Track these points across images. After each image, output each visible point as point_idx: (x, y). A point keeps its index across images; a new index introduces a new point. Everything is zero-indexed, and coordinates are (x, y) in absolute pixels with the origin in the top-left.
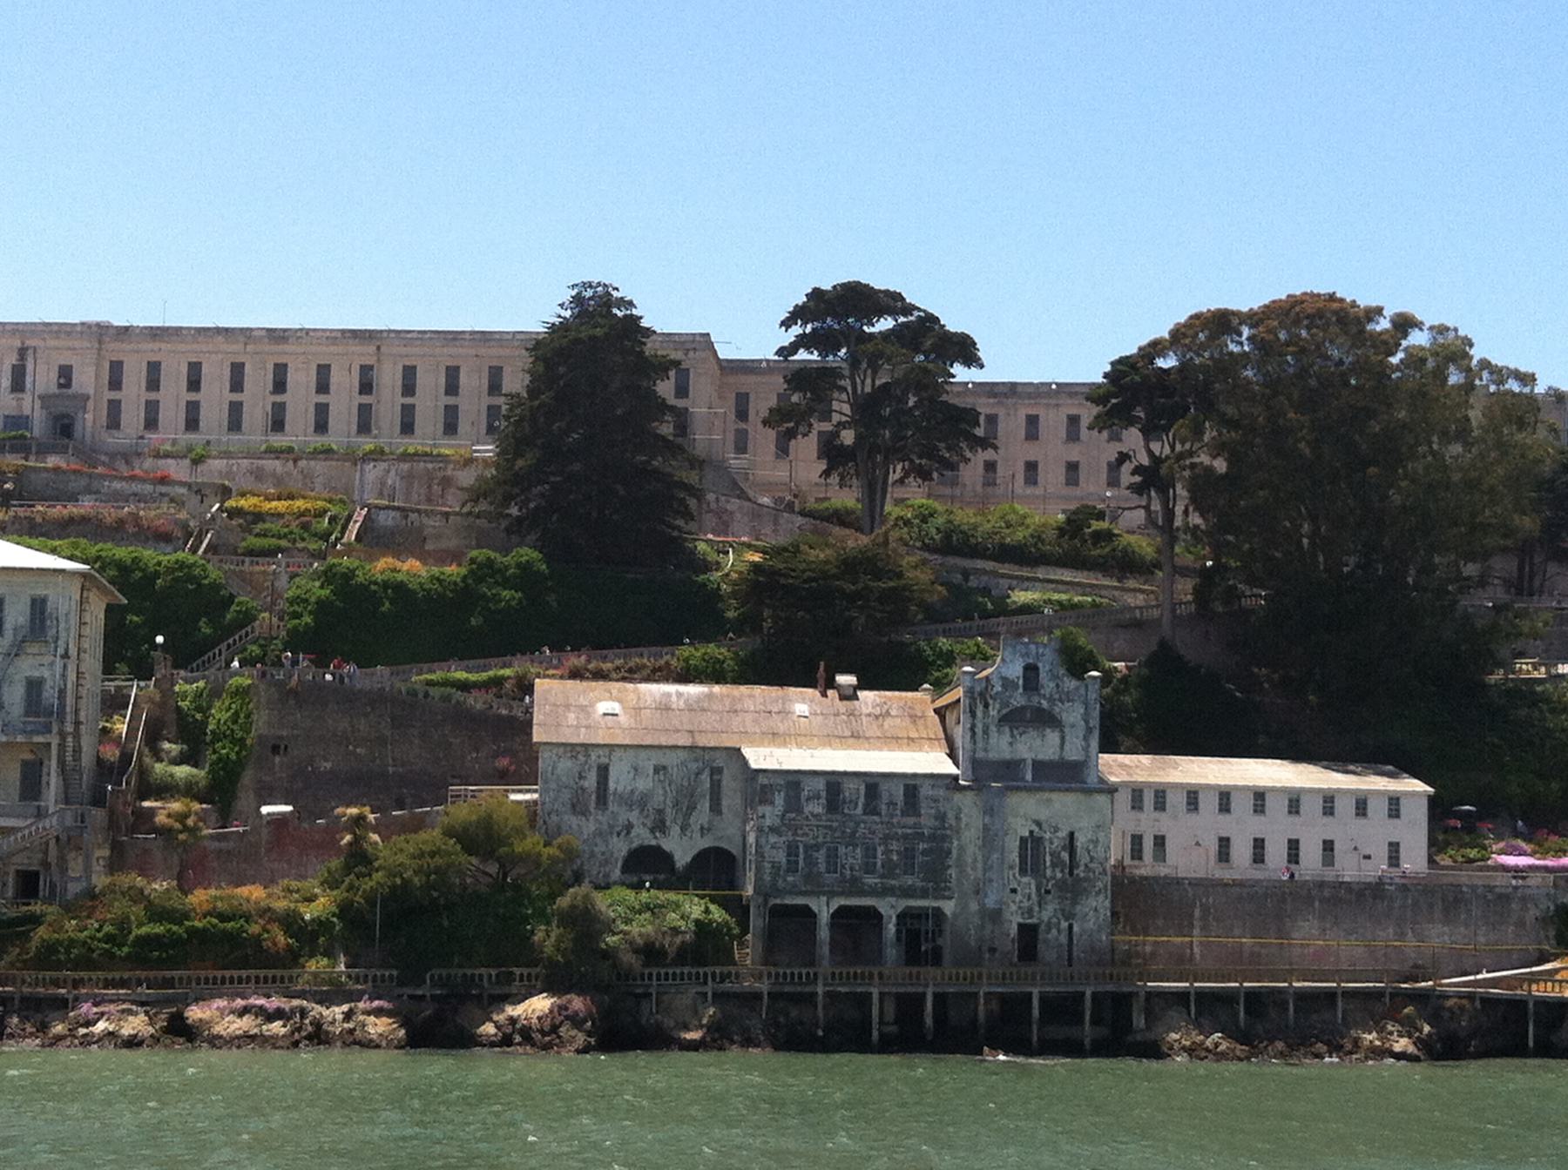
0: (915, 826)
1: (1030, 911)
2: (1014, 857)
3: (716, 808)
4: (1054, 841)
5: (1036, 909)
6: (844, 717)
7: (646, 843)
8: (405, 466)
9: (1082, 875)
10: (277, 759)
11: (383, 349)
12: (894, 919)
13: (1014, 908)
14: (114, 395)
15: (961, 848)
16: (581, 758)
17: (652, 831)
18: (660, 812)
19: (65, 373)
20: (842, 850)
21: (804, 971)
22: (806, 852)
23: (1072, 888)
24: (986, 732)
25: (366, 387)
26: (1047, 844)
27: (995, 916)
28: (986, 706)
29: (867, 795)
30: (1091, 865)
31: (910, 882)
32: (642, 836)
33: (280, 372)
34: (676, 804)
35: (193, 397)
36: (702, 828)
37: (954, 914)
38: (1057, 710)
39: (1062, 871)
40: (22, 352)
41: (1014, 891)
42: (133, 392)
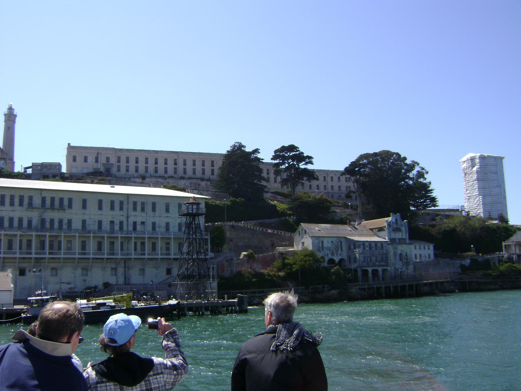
3: (341, 250)
4: (404, 254)
8: (190, 181)
10: (231, 243)
11: (179, 156)
14: (119, 164)
16: (319, 239)
17: (332, 255)
18: (333, 251)
19: (108, 159)
20: (372, 257)
23: (407, 264)
25: (175, 164)
32: (330, 256)
33: (156, 160)
35: (137, 165)
40: (98, 154)
42: (123, 164)
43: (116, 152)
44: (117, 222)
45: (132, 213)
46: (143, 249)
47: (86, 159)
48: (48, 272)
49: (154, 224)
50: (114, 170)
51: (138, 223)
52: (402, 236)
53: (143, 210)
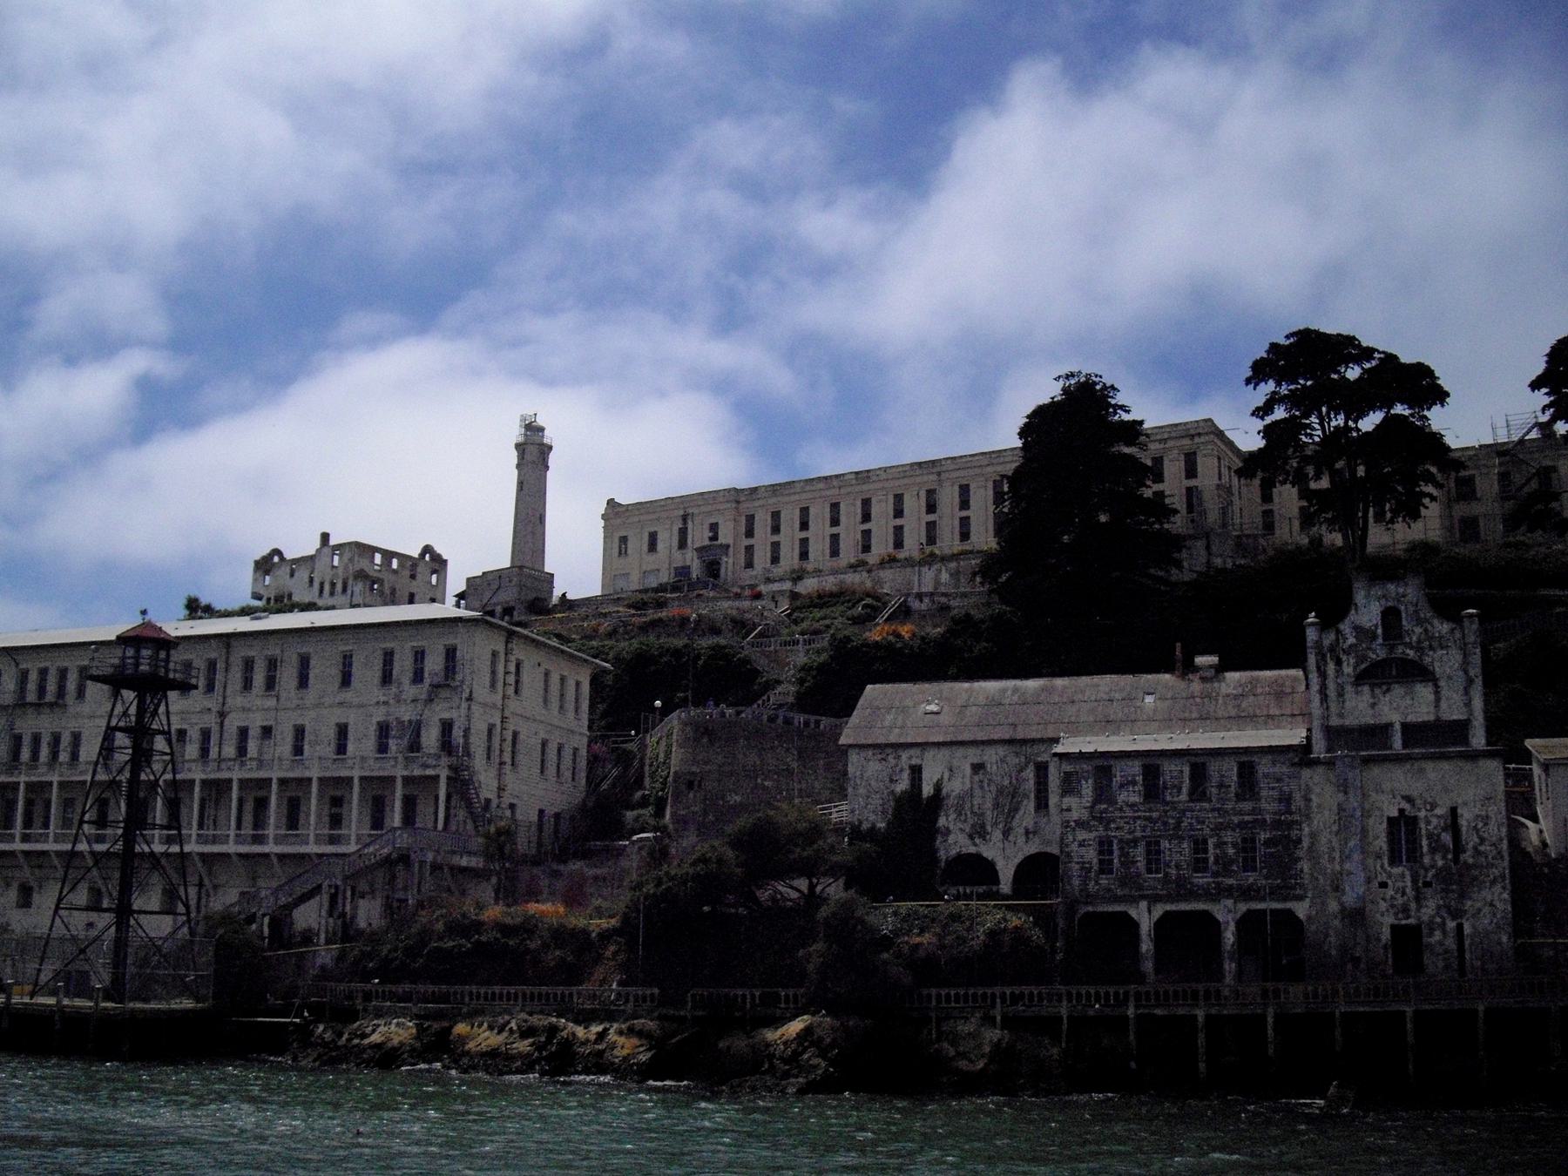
0: (1253, 811)
1: (1405, 910)
2: (1381, 843)
4: (1430, 822)
5: (1413, 906)
6: (1198, 700)
7: (964, 851)
8: (953, 565)
9: (1471, 861)
12: (1232, 927)
13: (1383, 905)
15: (1313, 835)
17: (971, 837)
19: (714, 527)
20: (1165, 844)
21: (1112, 991)
22: (1121, 849)
24: (1341, 695)
25: (931, 508)
26: (1423, 826)
27: (1356, 916)
28: (1339, 662)
29: (1192, 777)
30: (1482, 848)
31: (1251, 880)
34: (996, 805)
35: (804, 535)
36: (1027, 832)
37: (1309, 918)
38: (1427, 660)
39: (1444, 858)
40: (685, 518)
41: (1383, 885)
43: (738, 502)
44: (194, 734)
45: (236, 700)
46: (259, 822)
47: (652, 547)
48: (13, 894)
49: (300, 732)
50: (730, 565)
51: (254, 732)
52: (1437, 706)
53: (270, 684)
